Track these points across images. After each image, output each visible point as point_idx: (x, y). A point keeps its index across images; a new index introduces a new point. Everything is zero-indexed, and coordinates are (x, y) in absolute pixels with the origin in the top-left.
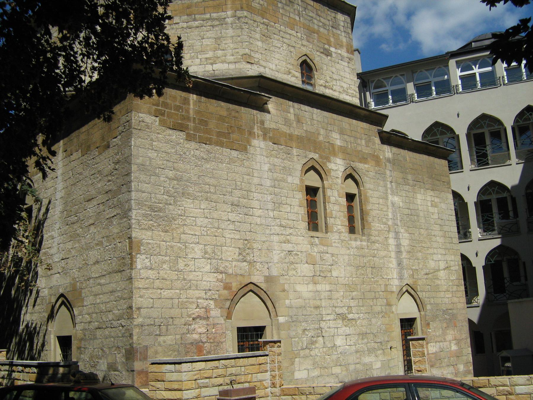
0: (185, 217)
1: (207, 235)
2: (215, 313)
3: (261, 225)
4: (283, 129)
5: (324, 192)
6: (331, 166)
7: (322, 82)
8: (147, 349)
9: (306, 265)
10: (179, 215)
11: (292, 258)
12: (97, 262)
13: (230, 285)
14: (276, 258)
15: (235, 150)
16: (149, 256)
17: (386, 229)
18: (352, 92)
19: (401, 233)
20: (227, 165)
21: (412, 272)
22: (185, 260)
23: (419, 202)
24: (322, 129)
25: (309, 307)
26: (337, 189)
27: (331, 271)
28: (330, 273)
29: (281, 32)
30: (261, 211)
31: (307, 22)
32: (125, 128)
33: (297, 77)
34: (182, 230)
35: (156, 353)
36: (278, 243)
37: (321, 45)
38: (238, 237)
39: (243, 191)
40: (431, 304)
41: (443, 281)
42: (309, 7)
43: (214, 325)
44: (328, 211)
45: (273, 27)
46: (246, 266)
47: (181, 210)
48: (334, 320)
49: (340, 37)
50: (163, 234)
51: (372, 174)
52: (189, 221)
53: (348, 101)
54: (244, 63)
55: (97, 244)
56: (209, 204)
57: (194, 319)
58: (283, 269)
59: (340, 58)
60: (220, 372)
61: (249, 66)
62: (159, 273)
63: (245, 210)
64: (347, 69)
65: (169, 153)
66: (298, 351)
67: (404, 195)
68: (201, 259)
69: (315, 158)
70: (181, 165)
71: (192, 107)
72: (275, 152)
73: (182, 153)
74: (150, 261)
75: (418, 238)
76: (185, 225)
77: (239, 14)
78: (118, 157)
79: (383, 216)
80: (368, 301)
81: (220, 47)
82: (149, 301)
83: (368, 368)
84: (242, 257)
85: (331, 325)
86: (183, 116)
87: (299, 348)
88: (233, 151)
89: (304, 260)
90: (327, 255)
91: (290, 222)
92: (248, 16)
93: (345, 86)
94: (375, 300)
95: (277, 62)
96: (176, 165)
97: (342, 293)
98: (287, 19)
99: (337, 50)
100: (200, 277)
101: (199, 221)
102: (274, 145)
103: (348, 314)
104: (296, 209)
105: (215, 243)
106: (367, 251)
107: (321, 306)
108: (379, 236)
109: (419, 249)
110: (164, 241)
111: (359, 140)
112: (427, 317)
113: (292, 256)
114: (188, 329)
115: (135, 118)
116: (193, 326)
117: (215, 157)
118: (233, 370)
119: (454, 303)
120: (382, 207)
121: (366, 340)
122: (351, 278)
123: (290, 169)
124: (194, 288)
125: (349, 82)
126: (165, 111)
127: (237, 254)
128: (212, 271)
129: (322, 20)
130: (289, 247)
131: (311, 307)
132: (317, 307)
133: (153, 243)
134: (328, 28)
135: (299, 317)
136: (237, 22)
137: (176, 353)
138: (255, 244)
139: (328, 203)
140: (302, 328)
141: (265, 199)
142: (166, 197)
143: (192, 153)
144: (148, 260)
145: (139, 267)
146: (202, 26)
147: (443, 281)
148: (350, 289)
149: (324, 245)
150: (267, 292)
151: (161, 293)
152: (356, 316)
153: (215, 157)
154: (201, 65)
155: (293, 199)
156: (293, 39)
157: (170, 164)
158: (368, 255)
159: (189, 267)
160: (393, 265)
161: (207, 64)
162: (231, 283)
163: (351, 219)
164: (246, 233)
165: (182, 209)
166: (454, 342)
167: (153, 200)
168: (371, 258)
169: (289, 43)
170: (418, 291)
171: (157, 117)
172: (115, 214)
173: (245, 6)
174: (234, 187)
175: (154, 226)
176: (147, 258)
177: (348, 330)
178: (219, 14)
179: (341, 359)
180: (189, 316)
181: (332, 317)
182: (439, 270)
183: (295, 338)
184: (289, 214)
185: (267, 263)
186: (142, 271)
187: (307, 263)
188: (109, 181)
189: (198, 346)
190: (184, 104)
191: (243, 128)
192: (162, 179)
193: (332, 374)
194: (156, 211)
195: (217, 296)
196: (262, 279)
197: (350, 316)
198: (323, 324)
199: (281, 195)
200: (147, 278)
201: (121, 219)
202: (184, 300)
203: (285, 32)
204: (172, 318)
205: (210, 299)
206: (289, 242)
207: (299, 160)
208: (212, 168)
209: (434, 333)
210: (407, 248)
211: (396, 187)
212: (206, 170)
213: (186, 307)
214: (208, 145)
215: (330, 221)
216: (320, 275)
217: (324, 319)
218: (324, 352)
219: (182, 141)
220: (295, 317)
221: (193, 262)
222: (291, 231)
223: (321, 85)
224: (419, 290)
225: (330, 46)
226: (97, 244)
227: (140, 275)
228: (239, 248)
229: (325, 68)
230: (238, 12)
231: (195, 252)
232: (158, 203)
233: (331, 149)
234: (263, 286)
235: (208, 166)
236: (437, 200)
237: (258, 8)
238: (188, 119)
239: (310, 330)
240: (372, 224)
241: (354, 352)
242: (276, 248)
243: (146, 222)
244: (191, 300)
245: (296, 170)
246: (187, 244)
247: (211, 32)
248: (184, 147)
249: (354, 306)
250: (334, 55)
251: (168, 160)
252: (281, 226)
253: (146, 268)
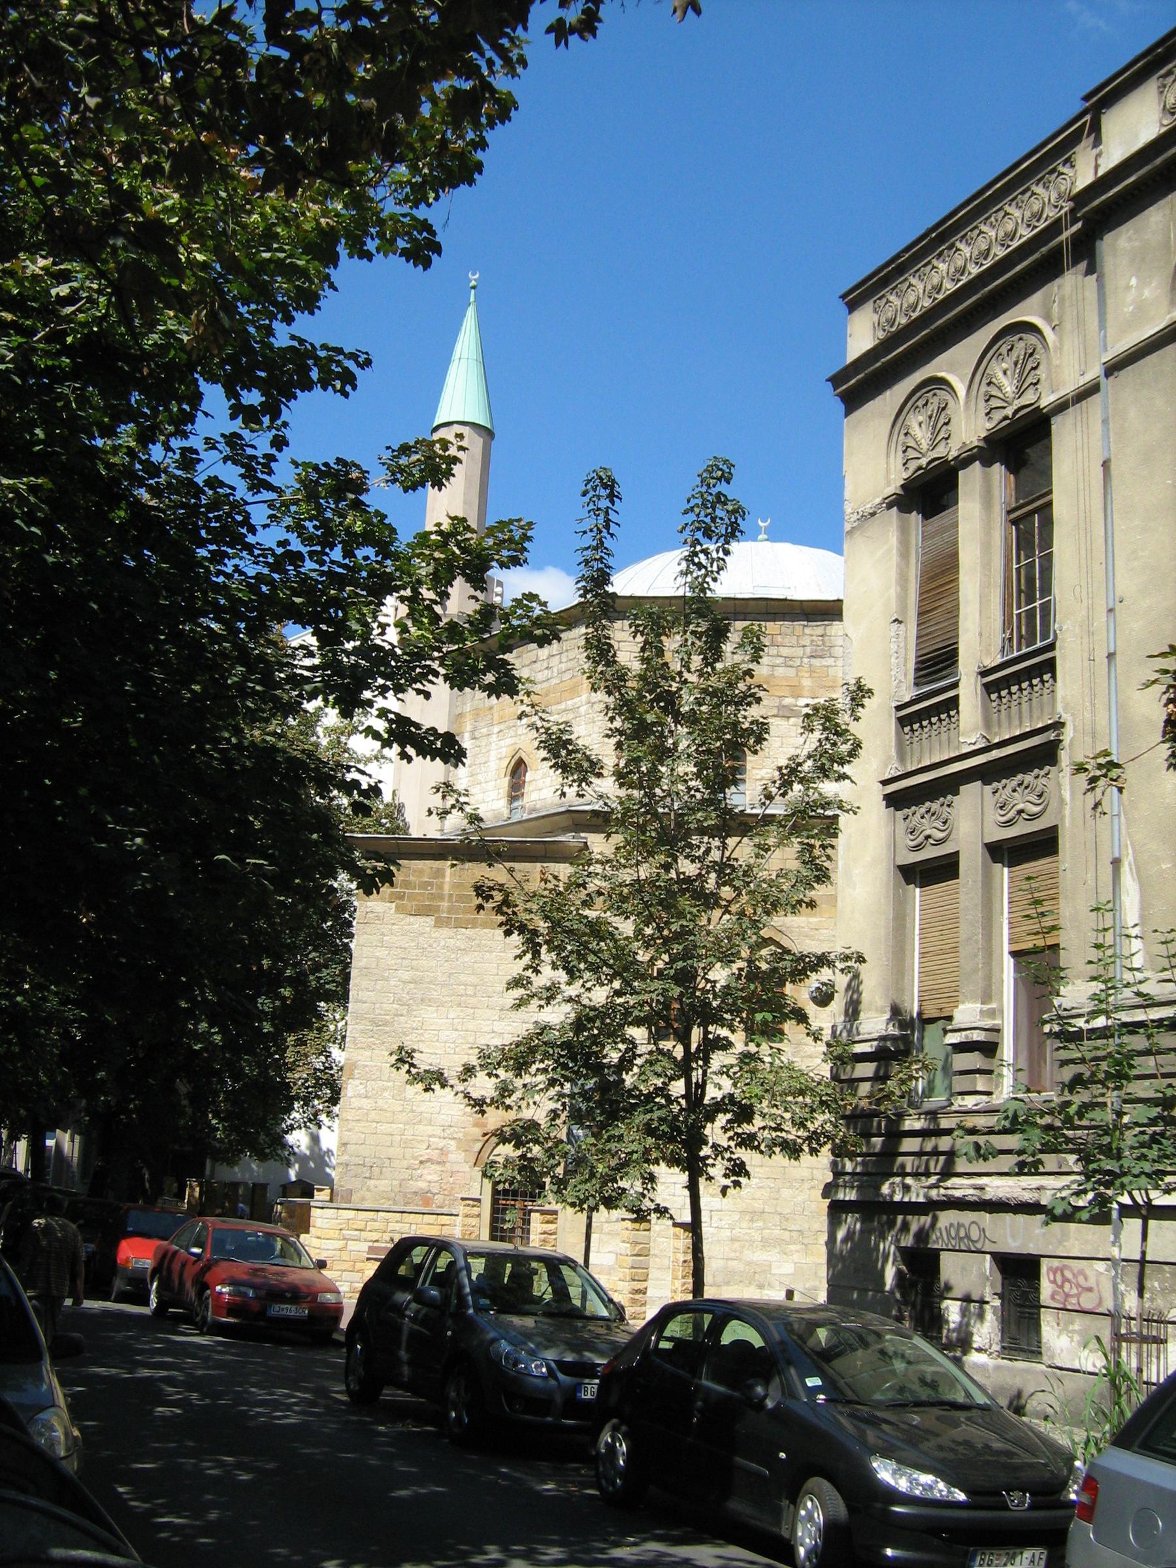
35: (363, 1199)
49: (832, 671)
57: (421, 1162)
60: (376, 1225)
70: (424, 963)
71: (447, 879)
83: (758, 1270)
96: (415, 963)
100: (437, 1109)
101: (443, 1036)
121: (760, 1224)
124: (425, 1122)
129: (784, 651)
143: (443, 943)
145: (349, 1094)
153: (479, 945)
157: (405, 962)
167: (377, 1011)
180: (415, 1158)
186: (353, 1100)
189: (426, 1197)
192: (392, 983)
195: (461, 1135)
200: (360, 1109)
225: (797, 697)
238: (441, 897)
253: (360, 1096)
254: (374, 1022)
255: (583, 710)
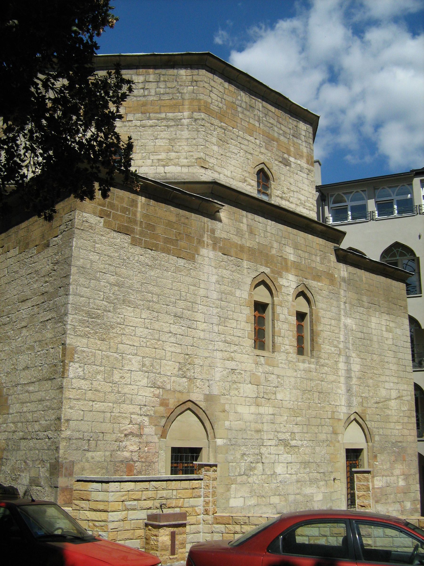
0: (124, 326)
1: (146, 347)
2: (150, 430)
3: (205, 339)
4: (234, 240)
5: (273, 309)
6: (282, 282)
7: (278, 193)
8: (73, 464)
9: (250, 385)
10: (118, 324)
11: (235, 376)
12: (27, 368)
13: (168, 402)
14: (218, 376)
15: (182, 258)
16: (82, 365)
17: (336, 352)
18: (310, 205)
19: (352, 357)
20: (172, 274)
21: (361, 400)
22: (121, 371)
23: (373, 325)
24: (275, 242)
25: (249, 430)
26: (287, 307)
27: (275, 394)
28: (274, 395)
29: (239, 138)
30: (205, 324)
31: (266, 129)
32: (67, 227)
33: (253, 186)
34: (119, 339)
35: (83, 469)
36: (221, 360)
37: (280, 154)
38: (179, 351)
39: (188, 303)
40: (379, 435)
41: (393, 411)
42: (270, 114)
43: (147, 443)
44: (276, 329)
45: (231, 131)
46: (186, 382)
47: (120, 318)
48: (275, 446)
49: (301, 147)
50: (99, 342)
51: (325, 293)
52: (127, 331)
53: (305, 215)
54: (198, 167)
55: (28, 349)
56: (150, 313)
57: (126, 435)
58: (225, 388)
59: (299, 169)
60: (150, 494)
61: (203, 170)
62: (92, 384)
63: (189, 323)
64: (306, 181)
65: (112, 257)
66: (235, 477)
67: (358, 317)
68: (138, 371)
69: (266, 273)
70: (123, 271)
71: (139, 209)
72: (224, 263)
73: (125, 258)
74: (84, 370)
75: (370, 364)
76: (123, 334)
77: (196, 115)
78: (57, 257)
79: (335, 339)
80: (313, 427)
81: (174, 149)
82: (80, 413)
83: (309, 500)
84: (182, 373)
85: (272, 452)
86: (129, 218)
87: (237, 474)
88: (180, 259)
89: (248, 380)
90: (272, 376)
91: (235, 339)
92: (206, 119)
93: (303, 198)
94: (320, 427)
95: (233, 168)
96: (118, 270)
97: (286, 417)
98: (246, 125)
99: (296, 160)
100: (136, 391)
102: (224, 256)
103: (291, 440)
104: (243, 325)
105: (154, 355)
106: (315, 374)
107: (263, 430)
108: (328, 359)
109: (370, 375)
110: (100, 350)
111: (314, 257)
112: (375, 449)
113: (235, 375)
114: (119, 446)
115: (78, 217)
116: (124, 443)
117: (160, 265)
118: (164, 493)
119: (404, 436)
120: (334, 328)
121: (308, 470)
122: (296, 403)
123: (239, 282)
124: (128, 402)
125: (307, 194)
126: (111, 212)
127: (177, 369)
128: (149, 385)
129: (283, 128)
130: (232, 365)
131: (252, 431)
132: (258, 431)
133: (88, 352)
134: (288, 137)
135: (238, 440)
136: (194, 124)
137: (104, 471)
138: (197, 360)
139: (277, 321)
140: (240, 452)
141: (211, 312)
142: (106, 303)
143: (137, 258)
144: (80, 370)
145: (71, 375)
146: (156, 126)
147: (393, 411)
148: (294, 414)
149: (269, 365)
150: (206, 412)
151: (92, 405)
152: (300, 443)
153: (160, 265)
154: (152, 166)
155: (240, 314)
156: (251, 145)
157: (112, 269)
158: (316, 378)
159: (124, 380)
160: (342, 390)
161: (159, 166)
162: (168, 400)
163: (300, 339)
164: (188, 347)
165: (122, 318)
166: (402, 477)
167: (92, 306)
168: (319, 382)
169: (246, 150)
170: (366, 421)
171: (102, 217)
172: (50, 317)
173: (202, 108)
174: (178, 297)
175: (90, 333)
176: (80, 367)
177: (289, 458)
178: (175, 114)
179: (280, 488)
180: (121, 432)
181: (273, 443)
182: (390, 399)
183: (233, 463)
184: (235, 330)
185: (208, 380)
186: (74, 381)
187: (250, 383)
188: (46, 282)
190: (132, 206)
191: (192, 235)
192: (102, 284)
193: (270, 504)
194: (93, 318)
195: (152, 413)
196: (201, 397)
197: (293, 443)
198: (263, 450)
199: (227, 309)
200: (79, 389)
201: (56, 323)
202: (117, 414)
203: (243, 138)
204: (103, 433)
205: (145, 416)
206: (232, 359)
207: (249, 273)
208: (156, 276)
209: (381, 467)
210: (357, 374)
211: (350, 308)
212: (149, 277)
213: (119, 422)
214: (153, 251)
215: (278, 340)
216: (263, 397)
217: (264, 444)
218: (262, 479)
219: (126, 245)
220: (235, 440)
221: (129, 375)
222: (236, 348)
223: (278, 196)
224: (368, 419)
225: (289, 155)
226: (28, 349)
227: (72, 385)
228: (180, 363)
229: (283, 178)
230: (195, 113)
231: (132, 364)
232: (97, 309)
233: (283, 264)
234: (202, 405)
235: (152, 274)
236: (392, 325)
237: (217, 111)
238: (135, 222)
239: (249, 455)
240: (322, 346)
241: (294, 481)
242: (218, 365)
243: (83, 329)
244: (124, 415)
245: (246, 284)
246: (124, 355)
247: (165, 132)
248: (128, 252)
249: (298, 433)
250: (293, 165)
251: (110, 265)
252: (225, 342)
254: (89, 314)
255: (185, 122)
